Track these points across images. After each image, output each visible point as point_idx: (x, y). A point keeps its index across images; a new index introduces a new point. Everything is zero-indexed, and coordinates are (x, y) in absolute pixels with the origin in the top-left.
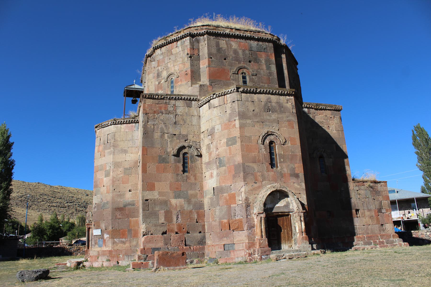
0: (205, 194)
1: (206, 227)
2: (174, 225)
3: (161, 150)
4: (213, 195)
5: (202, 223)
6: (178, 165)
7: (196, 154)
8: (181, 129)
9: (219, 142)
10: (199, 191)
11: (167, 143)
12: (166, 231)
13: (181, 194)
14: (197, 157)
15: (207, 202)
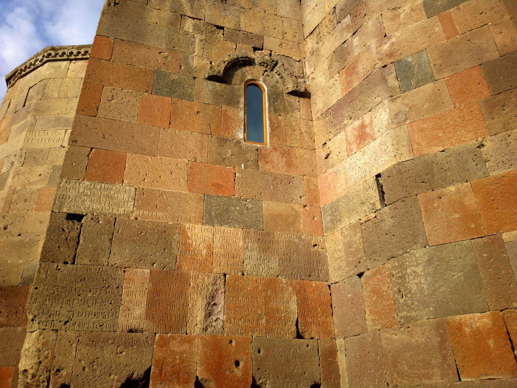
0: (327, 220)
1: (342, 360)
2: (190, 341)
3: (166, 57)
4: (378, 206)
5: (324, 344)
6: (226, 110)
7: (291, 87)
8: (242, 18)
9: (388, 14)
10: (305, 206)
11: (193, 43)
12: (148, 371)
13: (233, 208)
14: (294, 99)
15: (341, 246)
